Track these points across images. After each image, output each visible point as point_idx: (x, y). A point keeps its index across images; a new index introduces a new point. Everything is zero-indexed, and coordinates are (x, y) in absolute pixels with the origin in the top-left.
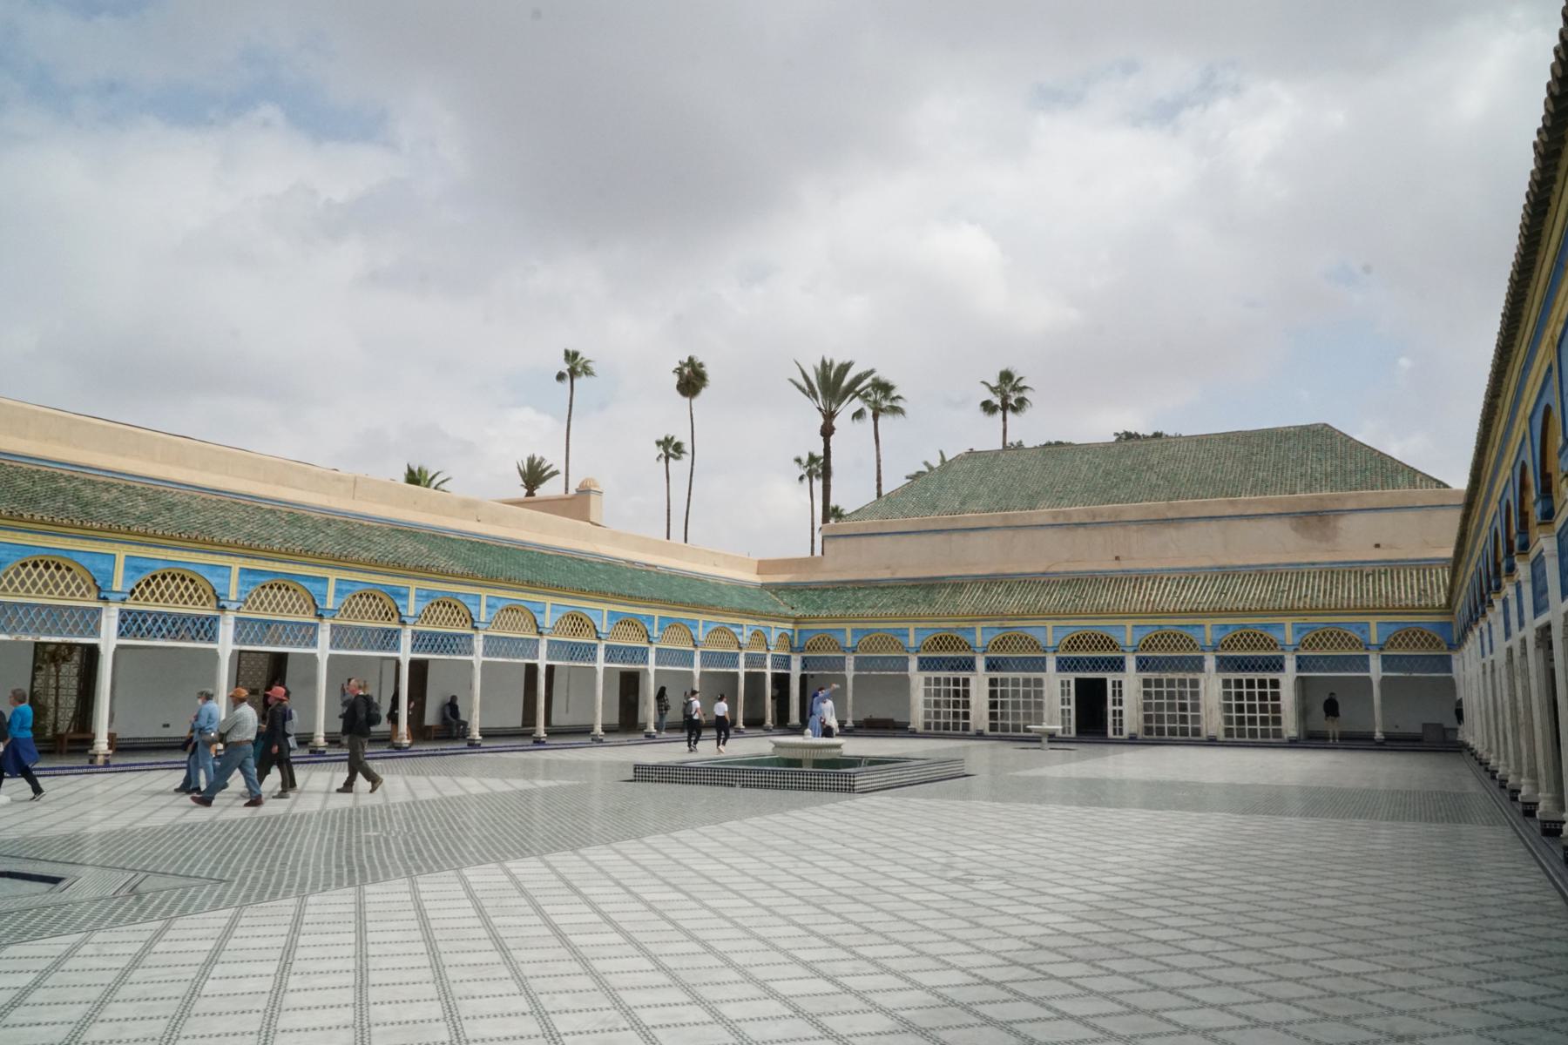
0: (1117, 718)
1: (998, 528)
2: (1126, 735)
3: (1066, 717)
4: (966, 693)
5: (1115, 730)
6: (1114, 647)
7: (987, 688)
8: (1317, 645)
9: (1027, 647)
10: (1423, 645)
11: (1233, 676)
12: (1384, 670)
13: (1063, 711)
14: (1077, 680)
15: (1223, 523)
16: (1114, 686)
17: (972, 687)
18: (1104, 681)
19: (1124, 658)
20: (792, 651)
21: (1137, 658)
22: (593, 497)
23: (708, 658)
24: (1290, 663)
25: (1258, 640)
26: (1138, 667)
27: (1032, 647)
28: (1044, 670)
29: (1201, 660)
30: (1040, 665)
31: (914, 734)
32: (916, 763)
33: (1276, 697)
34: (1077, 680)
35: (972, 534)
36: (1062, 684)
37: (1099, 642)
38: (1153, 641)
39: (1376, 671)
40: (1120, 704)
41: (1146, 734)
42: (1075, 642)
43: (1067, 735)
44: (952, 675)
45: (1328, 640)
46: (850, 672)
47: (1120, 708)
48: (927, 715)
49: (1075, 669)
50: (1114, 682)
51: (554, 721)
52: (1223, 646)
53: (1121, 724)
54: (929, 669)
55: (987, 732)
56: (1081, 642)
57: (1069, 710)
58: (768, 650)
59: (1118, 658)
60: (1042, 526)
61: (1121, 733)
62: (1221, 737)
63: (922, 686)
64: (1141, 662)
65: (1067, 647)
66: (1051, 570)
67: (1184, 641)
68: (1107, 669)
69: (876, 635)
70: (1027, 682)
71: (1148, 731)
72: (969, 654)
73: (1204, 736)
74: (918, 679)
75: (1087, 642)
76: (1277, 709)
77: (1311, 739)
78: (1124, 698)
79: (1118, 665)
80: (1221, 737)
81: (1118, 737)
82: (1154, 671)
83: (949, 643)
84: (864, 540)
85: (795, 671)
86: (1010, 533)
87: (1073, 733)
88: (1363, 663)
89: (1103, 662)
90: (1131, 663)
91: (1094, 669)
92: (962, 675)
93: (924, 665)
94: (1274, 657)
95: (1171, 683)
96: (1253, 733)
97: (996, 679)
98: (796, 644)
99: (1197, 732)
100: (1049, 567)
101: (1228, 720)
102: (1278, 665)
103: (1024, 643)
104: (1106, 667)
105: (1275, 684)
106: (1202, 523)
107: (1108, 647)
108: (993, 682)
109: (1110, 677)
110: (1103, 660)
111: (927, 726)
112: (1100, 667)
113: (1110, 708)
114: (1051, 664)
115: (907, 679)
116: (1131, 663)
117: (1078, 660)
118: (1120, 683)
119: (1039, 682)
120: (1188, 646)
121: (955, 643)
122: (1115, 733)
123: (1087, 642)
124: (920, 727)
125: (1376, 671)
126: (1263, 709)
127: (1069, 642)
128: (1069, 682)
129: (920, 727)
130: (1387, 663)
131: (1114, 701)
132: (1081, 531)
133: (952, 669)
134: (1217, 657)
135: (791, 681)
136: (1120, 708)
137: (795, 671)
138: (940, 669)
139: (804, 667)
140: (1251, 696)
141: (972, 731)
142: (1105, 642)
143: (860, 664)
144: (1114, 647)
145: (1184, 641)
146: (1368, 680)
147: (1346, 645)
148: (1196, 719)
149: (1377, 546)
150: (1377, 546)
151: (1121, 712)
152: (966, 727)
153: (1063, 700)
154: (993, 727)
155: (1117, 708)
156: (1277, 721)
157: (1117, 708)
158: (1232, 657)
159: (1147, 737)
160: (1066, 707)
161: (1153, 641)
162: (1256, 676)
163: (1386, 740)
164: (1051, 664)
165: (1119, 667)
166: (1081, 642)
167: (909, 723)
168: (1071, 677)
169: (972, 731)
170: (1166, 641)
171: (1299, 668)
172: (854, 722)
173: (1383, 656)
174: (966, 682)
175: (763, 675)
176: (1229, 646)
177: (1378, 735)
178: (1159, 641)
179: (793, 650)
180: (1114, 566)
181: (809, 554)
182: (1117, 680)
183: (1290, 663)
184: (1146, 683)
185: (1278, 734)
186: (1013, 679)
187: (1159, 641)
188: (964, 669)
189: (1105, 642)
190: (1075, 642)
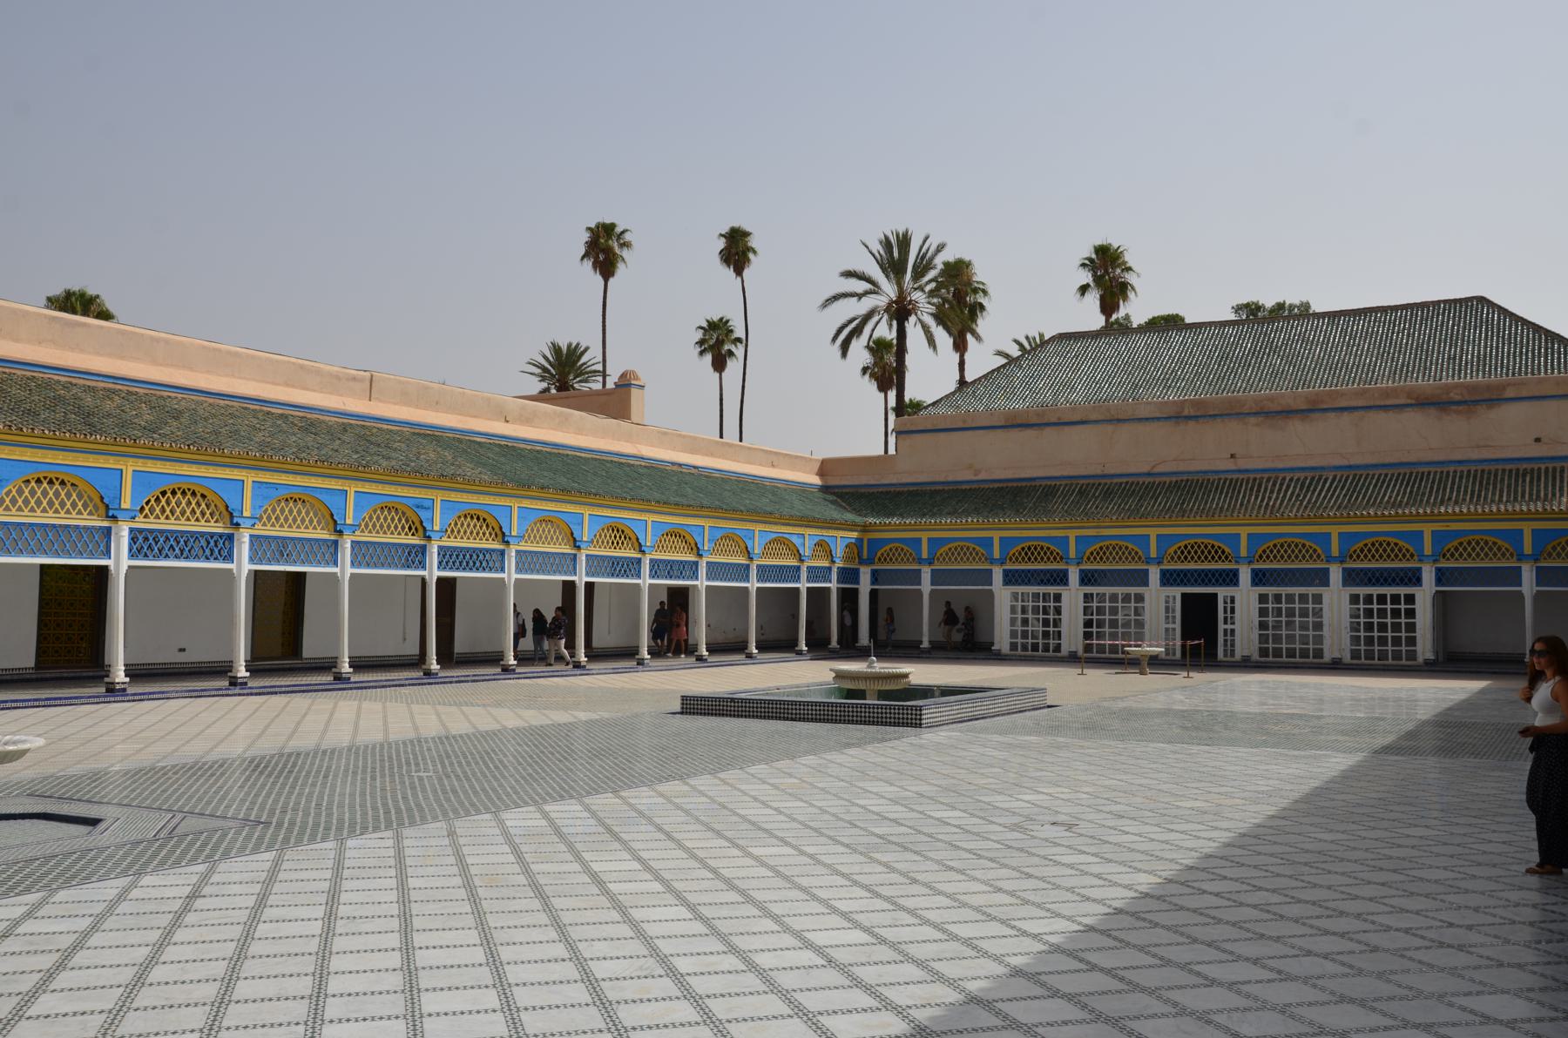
0: (1229, 638)
1: (1096, 422)
2: (1238, 657)
4: (1058, 611)
5: (1225, 651)
6: (1227, 558)
7: (1081, 605)
8: (1461, 555)
9: (1127, 558)
11: (1363, 591)
13: (1167, 630)
14: (1184, 596)
15: (1357, 414)
17: (1065, 603)
18: (1215, 595)
19: (1237, 570)
20: (860, 563)
21: (1253, 570)
22: (634, 391)
24: (1428, 575)
25: (1392, 550)
27: (1133, 558)
28: (1146, 584)
30: (1141, 578)
31: (998, 658)
32: (997, 692)
33: (1411, 613)
34: (1184, 596)
35: (1066, 428)
37: (1209, 552)
38: (1272, 551)
39: (1528, 585)
40: (1233, 623)
41: (1260, 656)
42: (1182, 552)
44: (1042, 589)
45: (1474, 549)
46: (926, 586)
47: (1232, 627)
48: (1013, 634)
49: (1182, 583)
50: (1225, 598)
51: (596, 643)
52: (1351, 557)
53: (1233, 645)
54: (1016, 583)
55: (1080, 652)
56: (1189, 552)
57: (1174, 629)
58: (833, 562)
59: (1231, 570)
60: (1147, 419)
61: (1233, 655)
62: (1347, 658)
64: (1257, 575)
65: (1172, 558)
66: (1157, 470)
67: (1307, 551)
68: (1218, 583)
69: (956, 544)
70: (1127, 598)
71: (1264, 652)
72: (1061, 566)
73: (1327, 658)
74: (1003, 597)
75: (1196, 552)
76: (1411, 627)
77: (1449, 662)
79: (1231, 578)
81: (1229, 659)
82: (1271, 585)
83: (1039, 553)
84: (942, 435)
85: (865, 586)
86: (1110, 428)
87: (1178, 655)
88: (1514, 576)
90: (1245, 575)
91: (1204, 583)
92: (1052, 590)
93: (1011, 578)
94: (1410, 569)
95: (1290, 599)
96: (1383, 655)
97: (1092, 595)
98: (865, 555)
99: (1319, 653)
100: (1154, 467)
101: (1355, 640)
102: (1414, 578)
103: (1123, 553)
105: (1410, 599)
106: (1332, 415)
107: (1220, 558)
108: (1088, 597)
109: (1222, 592)
110: (1213, 572)
111: (1013, 646)
113: (1221, 626)
114: (1154, 574)
115: (991, 594)
116: (1245, 575)
117: (1185, 573)
118: (1233, 601)
119: (1140, 598)
120: (1311, 557)
121: (1045, 553)
122: (1225, 656)
123: (1196, 552)
125: (1528, 585)
126: (1396, 627)
127: (1175, 552)
128: (1174, 598)
129: (1006, 649)
130: (1543, 576)
131: (1226, 619)
132: (1191, 424)
133: (1042, 583)
136: (1232, 627)
137: (865, 586)
138: (1029, 583)
140: (1382, 613)
141: (1065, 651)
142: (1216, 552)
143: (937, 577)
144: (1227, 558)
145: (1307, 551)
146: (1520, 595)
147: (1495, 555)
148: (1319, 639)
150: (1538, 440)
151: (1233, 631)
152: (1058, 648)
153: (1167, 618)
154: (1088, 648)
156: (1412, 641)
158: (1362, 569)
159: (1263, 659)
160: (1171, 626)
161: (1272, 551)
162: (1388, 591)
165: (1231, 580)
166: (1189, 552)
167: (992, 644)
168: (1177, 592)
169: (1065, 651)
170: (1286, 551)
171: (1439, 582)
172: (930, 642)
173: (1537, 567)
174: (1058, 598)
176: (1358, 556)
178: (1279, 551)
179: (862, 562)
180: (1230, 465)
181: (882, 453)
183: (1428, 575)
184: (1263, 598)
185: (1412, 655)
187: (1279, 551)
189: (1216, 552)
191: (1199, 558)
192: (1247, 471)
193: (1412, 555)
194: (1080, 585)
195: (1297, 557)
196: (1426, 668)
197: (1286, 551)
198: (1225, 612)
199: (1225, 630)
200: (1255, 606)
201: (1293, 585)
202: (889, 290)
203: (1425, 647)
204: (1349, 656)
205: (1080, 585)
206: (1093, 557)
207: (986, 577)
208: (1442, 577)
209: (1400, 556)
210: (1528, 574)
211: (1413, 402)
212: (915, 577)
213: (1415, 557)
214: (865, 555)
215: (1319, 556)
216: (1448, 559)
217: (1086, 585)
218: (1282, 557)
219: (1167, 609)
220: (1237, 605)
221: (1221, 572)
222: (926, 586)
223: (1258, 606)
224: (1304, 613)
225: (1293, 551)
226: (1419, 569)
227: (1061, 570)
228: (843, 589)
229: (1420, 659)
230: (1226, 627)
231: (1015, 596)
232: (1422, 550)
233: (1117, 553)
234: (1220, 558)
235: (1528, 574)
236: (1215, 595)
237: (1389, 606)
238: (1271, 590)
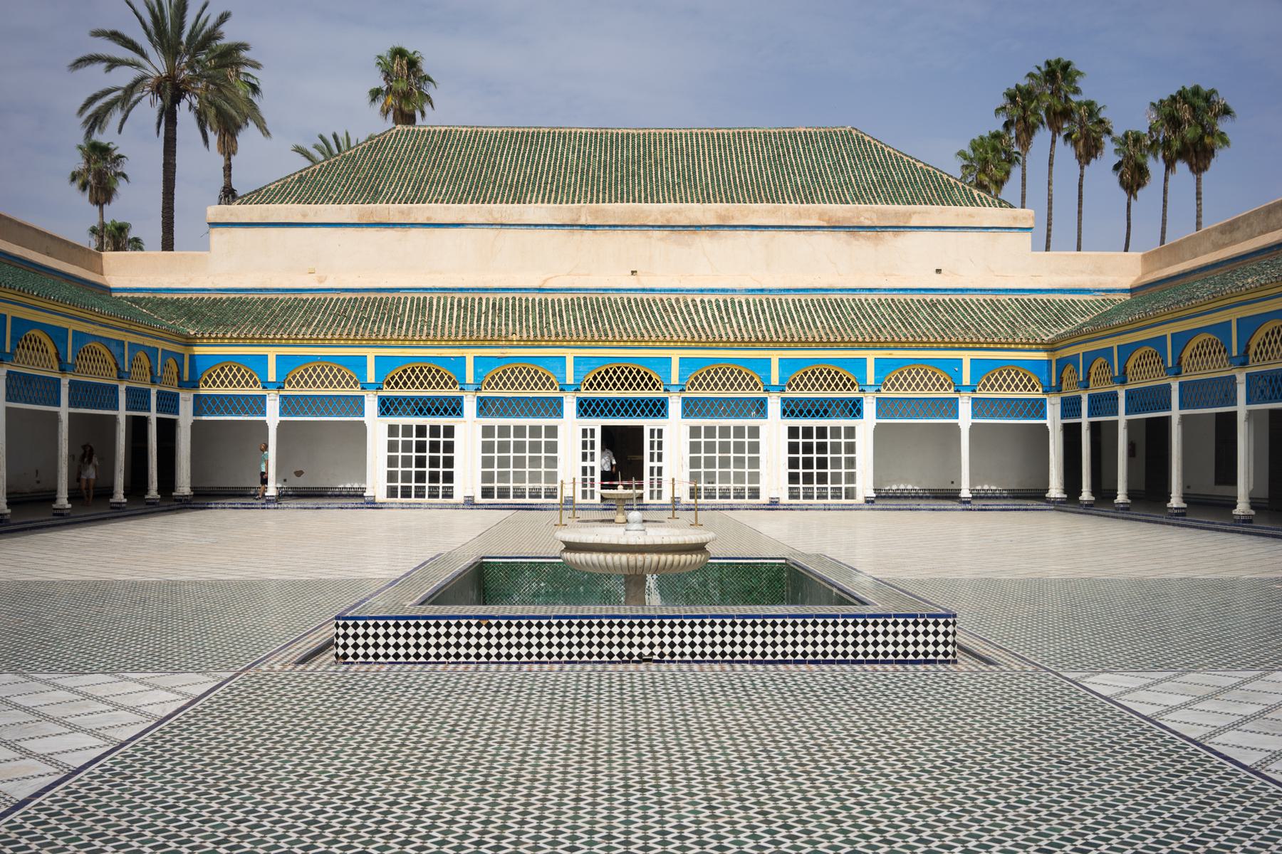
3: (589, 477)
4: (449, 447)
5: (652, 492)
6: (654, 385)
7: (479, 439)
10: (1017, 387)
11: (801, 423)
12: (878, 417)
14: (604, 428)
16: (652, 436)
17: (458, 440)
18: (640, 429)
20: (180, 386)
21: (684, 399)
23: (1135, 400)
24: (869, 407)
26: (684, 411)
29: (559, 402)
30: (555, 408)
31: (373, 504)
33: (851, 448)
34: (604, 428)
36: (584, 431)
39: (965, 418)
40: (660, 459)
42: (603, 379)
43: (588, 501)
44: (415, 421)
46: (273, 416)
48: (391, 477)
50: (652, 431)
55: (479, 499)
60: (536, 225)
61: (659, 497)
63: (384, 439)
65: (591, 385)
72: (454, 393)
74: (377, 427)
75: (619, 378)
78: (665, 451)
79: (658, 408)
80: (785, 499)
81: (655, 501)
82: (704, 416)
83: (425, 377)
88: (951, 407)
89: (638, 405)
90: (675, 406)
92: (442, 421)
93: (386, 407)
98: (186, 377)
100: (545, 281)
101: (793, 478)
102: (854, 409)
103: (532, 378)
104: (643, 411)
105: (851, 432)
107: (646, 385)
108: (487, 431)
109: (648, 424)
110: (639, 402)
111: (392, 492)
112: (635, 411)
113: (647, 464)
114: (570, 405)
115: (360, 431)
116: (675, 406)
117: (606, 402)
118: (660, 432)
119: (552, 431)
122: (652, 498)
123: (619, 378)
124: (381, 496)
125: (965, 418)
128: (592, 431)
129: (381, 496)
130: (980, 407)
134: (783, 400)
135: (178, 430)
136: (660, 464)
137: (185, 417)
138: (405, 413)
139: (197, 411)
142: (642, 379)
143: (288, 405)
144: (654, 385)
149: (938, 271)
151: (660, 469)
154: (487, 493)
155: (656, 464)
156: (851, 478)
157: (656, 464)
163: (973, 498)
164: (570, 405)
165: (659, 411)
168: (597, 424)
169: (458, 497)
170: (720, 379)
171: (880, 414)
173: (684, 399)
174: (449, 431)
175: (114, 418)
177: (965, 493)
179: (182, 385)
180: (632, 283)
182: (656, 428)
183: (869, 407)
184: (695, 432)
185: (850, 494)
186: (418, 427)
188: (446, 412)
189: (642, 379)
190: (603, 379)
191: (622, 385)
192: (652, 290)
193: (853, 385)
194: (478, 416)
195: (732, 385)
196: (867, 506)
197: (720, 379)
198: (652, 447)
199: (652, 469)
200: (686, 440)
201: (729, 416)
202: (157, 64)
203: (865, 486)
204: (787, 495)
205: (478, 416)
206: (492, 383)
207: (356, 405)
208: (884, 407)
209: (619, 385)
210: (965, 407)
211: (825, 224)
212: (258, 404)
213: (856, 387)
214: (186, 377)
215: (756, 385)
216: (889, 389)
217: (485, 415)
218: (716, 385)
219: (584, 445)
220: (666, 439)
221: (647, 402)
222: (273, 416)
223: (689, 440)
224: (739, 447)
225: (728, 379)
226: (859, 400)
227: (454, 398)
228: (134, 417)
229: (860, 499)
230: (652, 464)
231: (393, 430)
232: (769, 379)
233: (524, 378)
234: (646, 385)
235: (965, 407)
236: (640, 429)
237: (717, 440)
238: (703, 422)
